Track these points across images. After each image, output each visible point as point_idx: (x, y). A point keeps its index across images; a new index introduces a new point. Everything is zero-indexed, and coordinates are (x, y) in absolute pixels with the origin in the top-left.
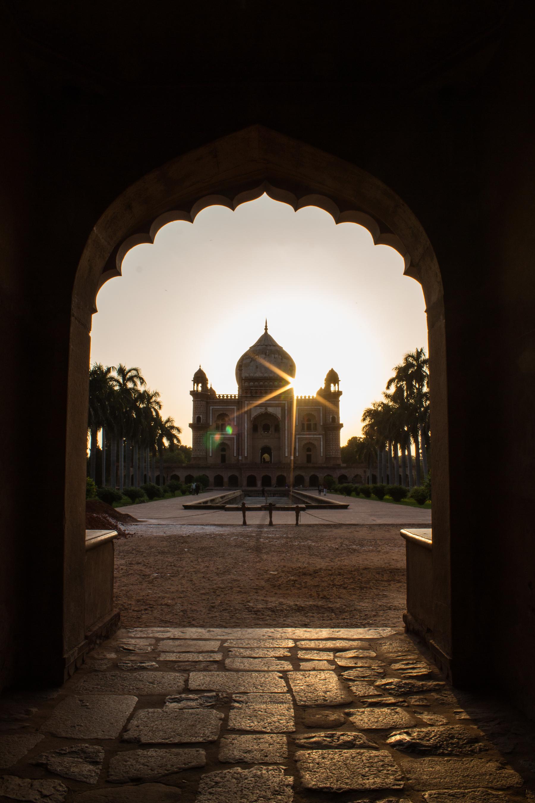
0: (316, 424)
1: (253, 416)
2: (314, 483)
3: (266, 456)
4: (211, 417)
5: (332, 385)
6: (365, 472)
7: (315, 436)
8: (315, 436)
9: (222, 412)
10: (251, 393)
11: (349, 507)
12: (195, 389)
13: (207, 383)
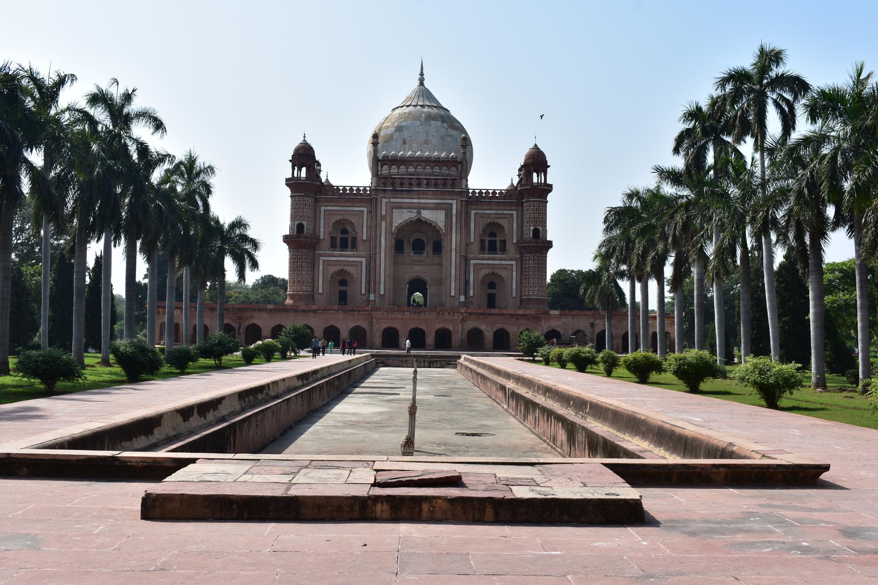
0: (504, 242)
1: (395, 225)
2: (502, 343)
3: (418, 294)
4: (322, 225)
5: (535, 175)
6: (592, 325)
7: (503, 262)
8: (503, 262)
9: (341, 217)
10: (393, 184)
11: (825, 476)
12: (296, 175)
13: (320, 171)
